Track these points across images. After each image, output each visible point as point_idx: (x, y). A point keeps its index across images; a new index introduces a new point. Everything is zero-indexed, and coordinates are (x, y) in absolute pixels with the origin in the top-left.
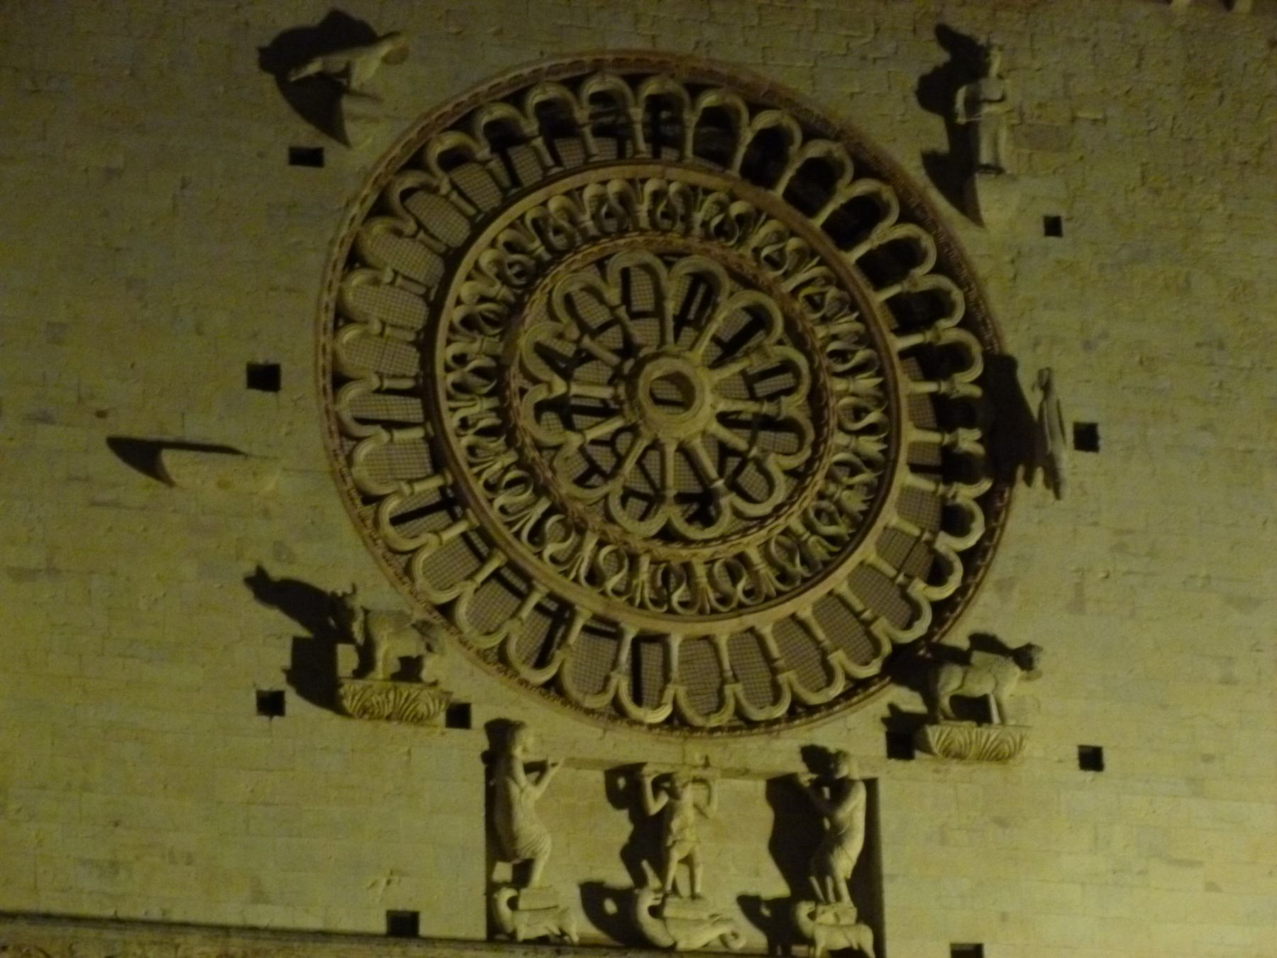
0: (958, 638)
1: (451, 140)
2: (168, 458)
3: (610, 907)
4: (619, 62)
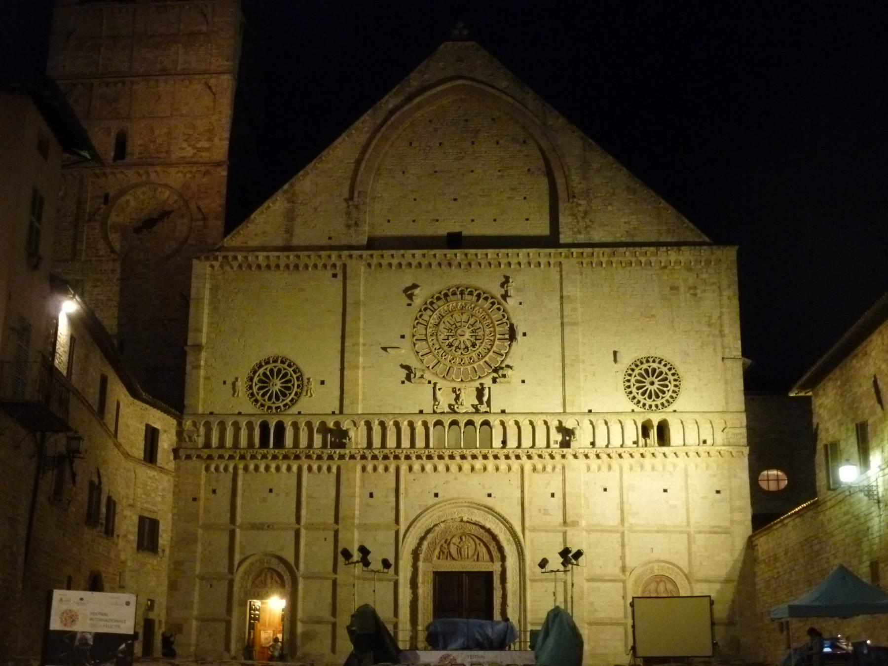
0: (503, 365)
1: (430, 300)
2: (388, 350)
3: (452, 407)
4: (455, 286)
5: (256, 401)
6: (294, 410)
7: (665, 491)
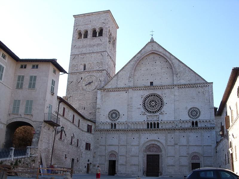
5: (110, 119)
6: (118, 121)
7: (197, 137)
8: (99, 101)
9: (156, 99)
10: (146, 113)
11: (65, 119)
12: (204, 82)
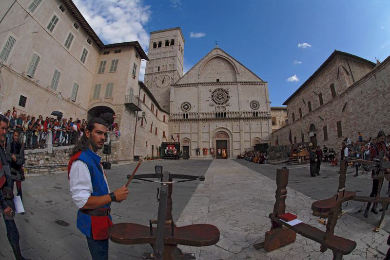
8: (172, 95)
9: (223, 93)
10: (215, 104)
11: (145, 105)
12: (260, 81)
